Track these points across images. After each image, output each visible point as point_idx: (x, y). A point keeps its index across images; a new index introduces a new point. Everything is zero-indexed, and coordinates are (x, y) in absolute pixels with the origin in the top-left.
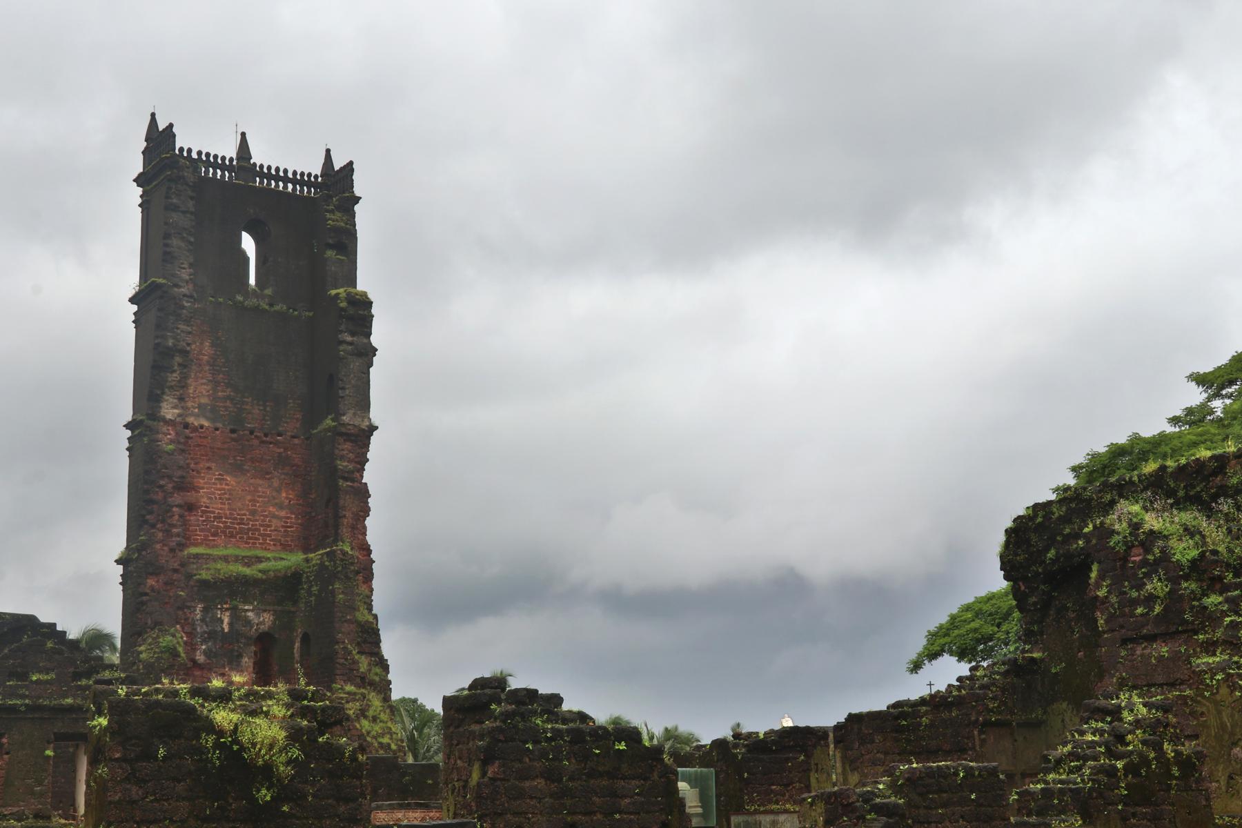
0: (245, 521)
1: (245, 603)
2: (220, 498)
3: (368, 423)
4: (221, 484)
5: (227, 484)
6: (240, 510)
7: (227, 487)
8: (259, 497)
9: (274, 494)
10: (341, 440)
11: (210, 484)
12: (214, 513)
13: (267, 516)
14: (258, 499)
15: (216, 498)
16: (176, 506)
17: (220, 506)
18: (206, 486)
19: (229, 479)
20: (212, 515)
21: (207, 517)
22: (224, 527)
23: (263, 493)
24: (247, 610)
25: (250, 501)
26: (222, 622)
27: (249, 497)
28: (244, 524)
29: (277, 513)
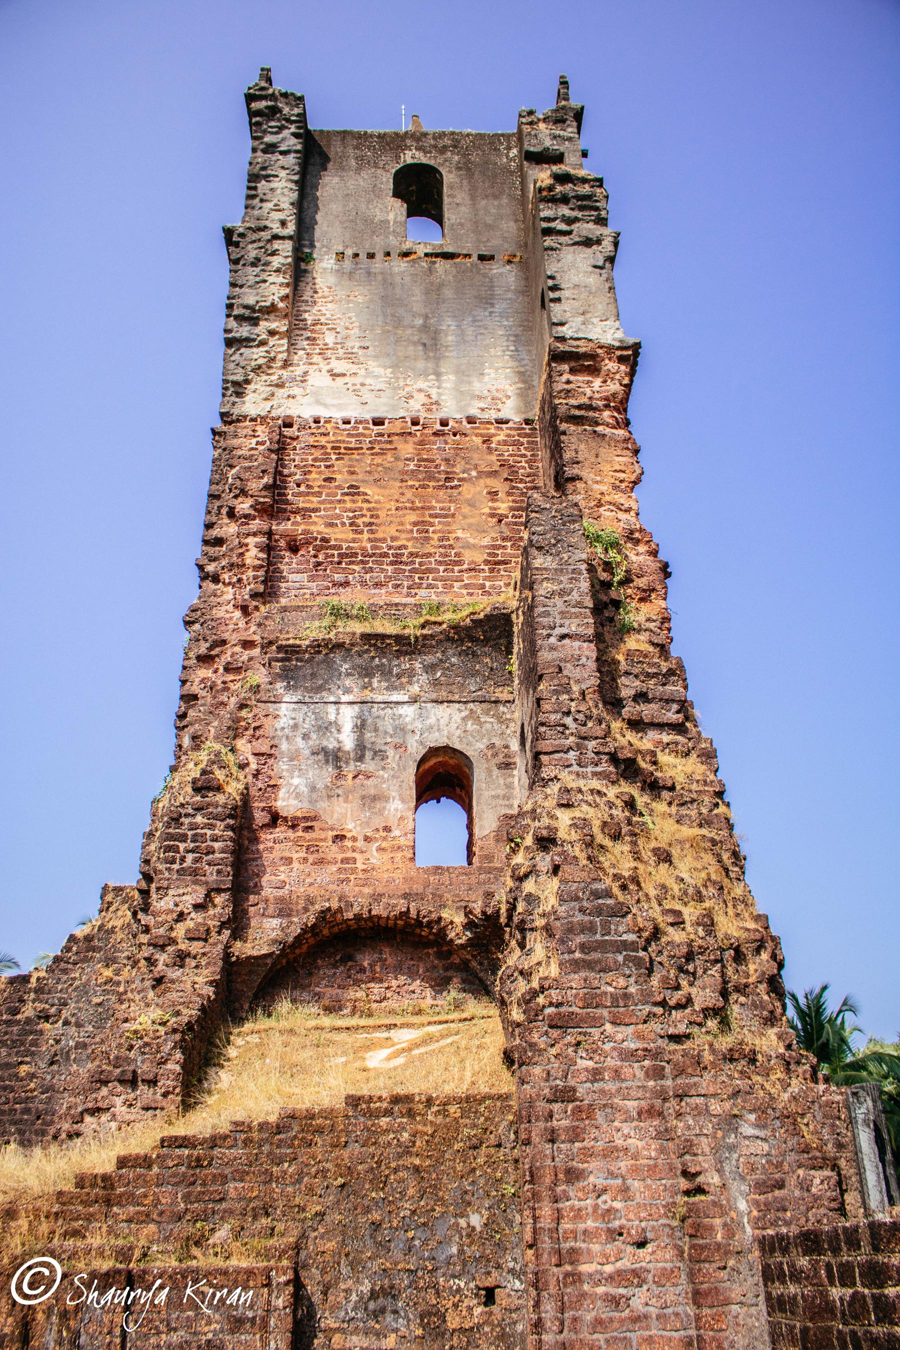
0: (405, 559)
1: (391, 688)
2: (351, 525)
4: (354, 502)
5: (368, 501)
7: (365, 505)
9: (466, 510)
11: (331, 502)
12: (340, 547)
14: (432, 520)
15: (343, 524)
16: (255, 534)
17: (351, 536)
18: (322, 507)
19: (369, 492)
20: (336, 552)
21: (327, 556)
23: (442, 509)
25: (415, 524)
27: (413, 517)
28: (406, 564)
29: (472, 541)
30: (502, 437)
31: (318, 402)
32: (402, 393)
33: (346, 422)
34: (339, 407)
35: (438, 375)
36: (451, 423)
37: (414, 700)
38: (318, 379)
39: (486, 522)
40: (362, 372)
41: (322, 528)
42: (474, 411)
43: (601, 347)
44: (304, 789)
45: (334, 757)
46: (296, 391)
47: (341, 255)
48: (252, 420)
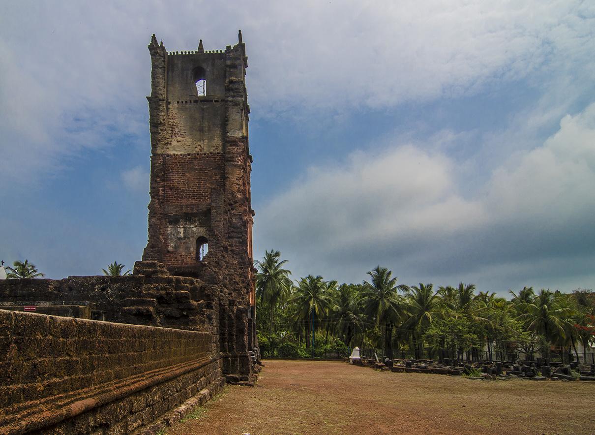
1: (191, 224)
3: (241, 135)
6: (193, 187)
8: (202, 180)
10: (229, 145)
12: (180, 189)
13: (206, 188)
22: (186, 195)
24: (192, 227)
25: (197, 183)
26: (180, 233)
30: (218, 158)
31: (175, 150)
32: (194, 146)
33: (181, 155)
34: (179, 151)
35: (203, 140)
36: (206, 155)
37: (196, 226)
38: (174, 143)
39: (214, 182)
40: (185, 140)
41: (176, 184)
42: (212, 151)
43: (237, 138)
44: (174, 246)
45: (180, 239)
46: (169, 146)
47: (178, 102)
48: (159, 155)
